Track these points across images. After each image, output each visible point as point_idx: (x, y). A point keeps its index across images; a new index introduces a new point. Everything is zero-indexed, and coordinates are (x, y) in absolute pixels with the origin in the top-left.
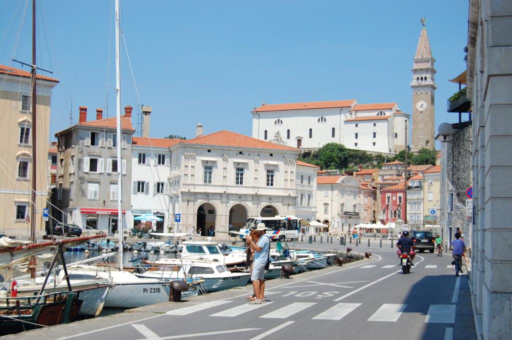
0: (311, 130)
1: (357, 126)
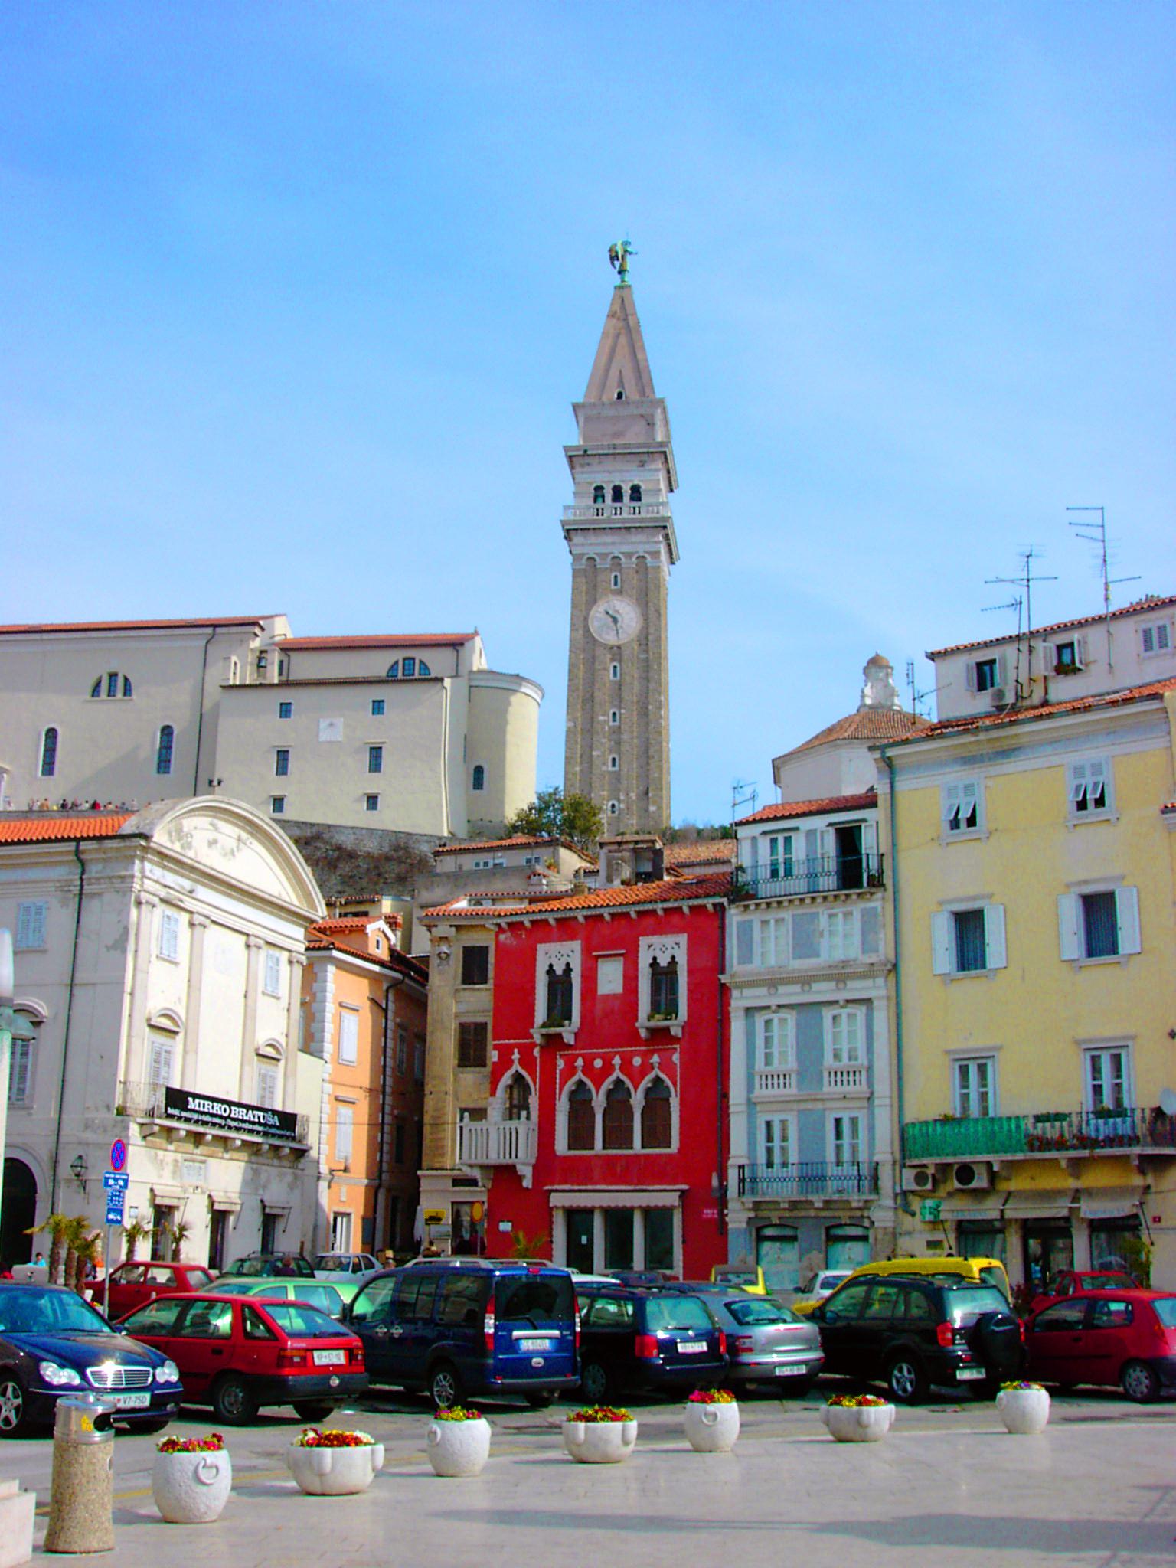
0: (52, 734)
1: (285, 710)
